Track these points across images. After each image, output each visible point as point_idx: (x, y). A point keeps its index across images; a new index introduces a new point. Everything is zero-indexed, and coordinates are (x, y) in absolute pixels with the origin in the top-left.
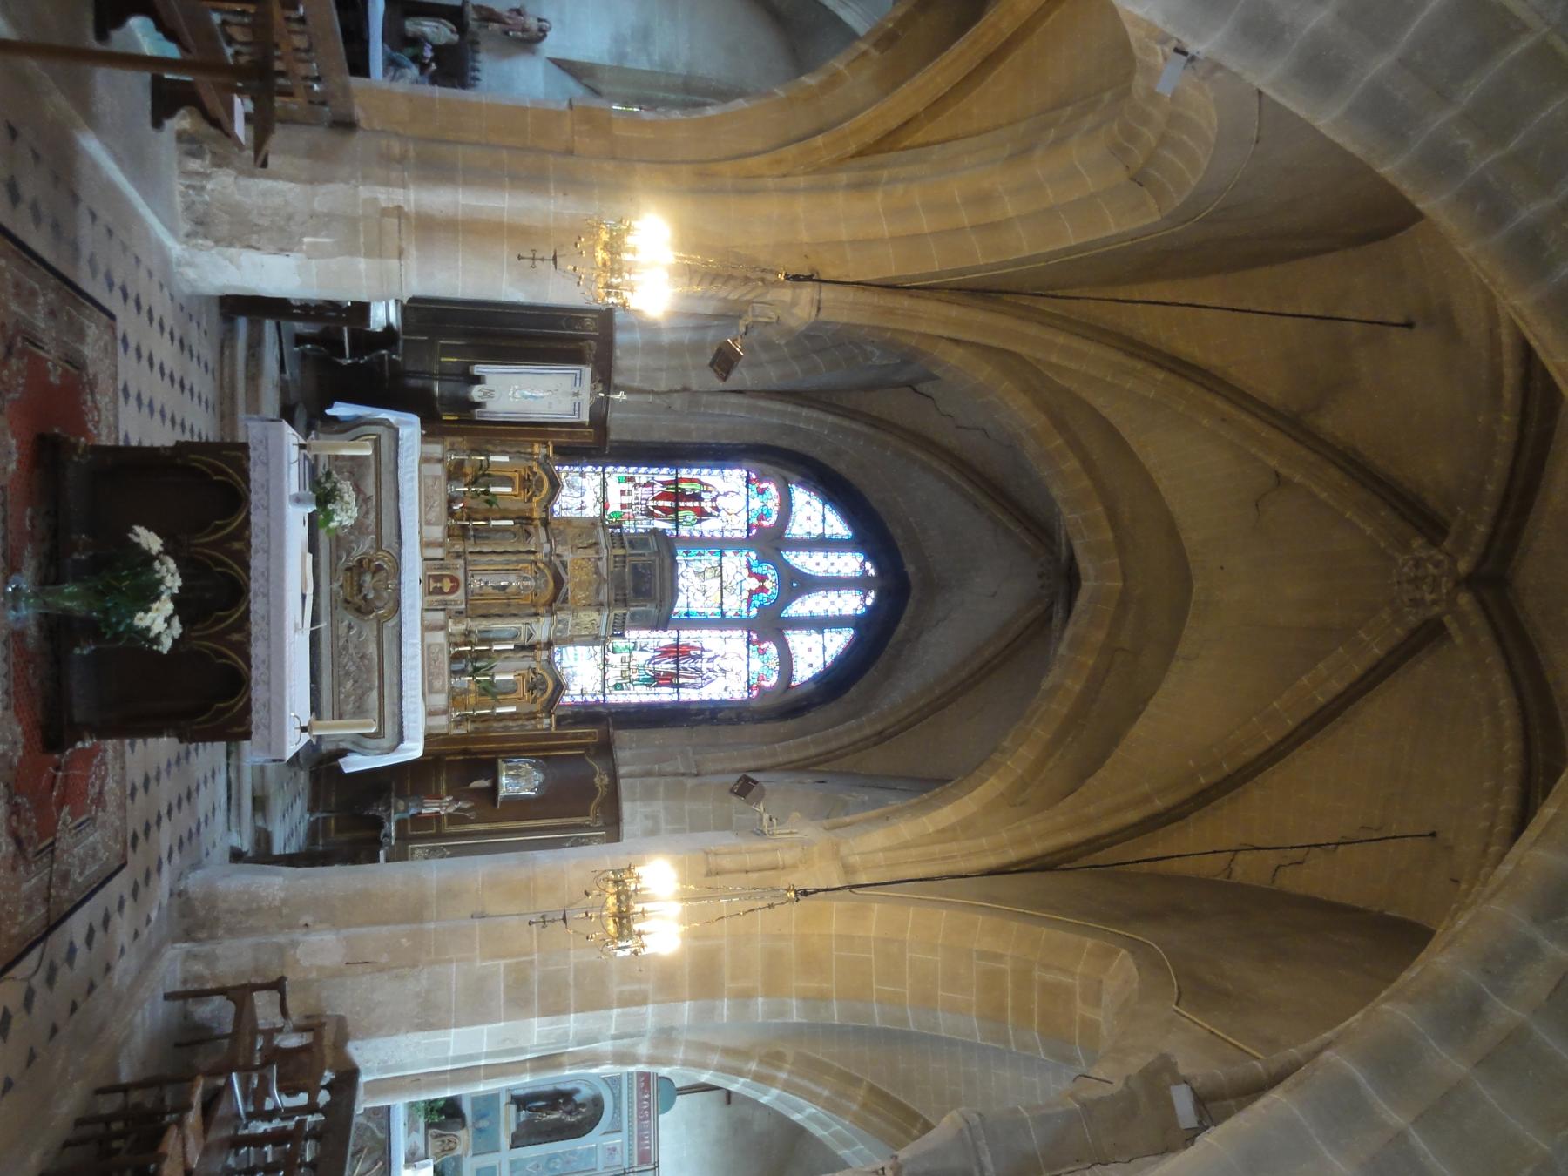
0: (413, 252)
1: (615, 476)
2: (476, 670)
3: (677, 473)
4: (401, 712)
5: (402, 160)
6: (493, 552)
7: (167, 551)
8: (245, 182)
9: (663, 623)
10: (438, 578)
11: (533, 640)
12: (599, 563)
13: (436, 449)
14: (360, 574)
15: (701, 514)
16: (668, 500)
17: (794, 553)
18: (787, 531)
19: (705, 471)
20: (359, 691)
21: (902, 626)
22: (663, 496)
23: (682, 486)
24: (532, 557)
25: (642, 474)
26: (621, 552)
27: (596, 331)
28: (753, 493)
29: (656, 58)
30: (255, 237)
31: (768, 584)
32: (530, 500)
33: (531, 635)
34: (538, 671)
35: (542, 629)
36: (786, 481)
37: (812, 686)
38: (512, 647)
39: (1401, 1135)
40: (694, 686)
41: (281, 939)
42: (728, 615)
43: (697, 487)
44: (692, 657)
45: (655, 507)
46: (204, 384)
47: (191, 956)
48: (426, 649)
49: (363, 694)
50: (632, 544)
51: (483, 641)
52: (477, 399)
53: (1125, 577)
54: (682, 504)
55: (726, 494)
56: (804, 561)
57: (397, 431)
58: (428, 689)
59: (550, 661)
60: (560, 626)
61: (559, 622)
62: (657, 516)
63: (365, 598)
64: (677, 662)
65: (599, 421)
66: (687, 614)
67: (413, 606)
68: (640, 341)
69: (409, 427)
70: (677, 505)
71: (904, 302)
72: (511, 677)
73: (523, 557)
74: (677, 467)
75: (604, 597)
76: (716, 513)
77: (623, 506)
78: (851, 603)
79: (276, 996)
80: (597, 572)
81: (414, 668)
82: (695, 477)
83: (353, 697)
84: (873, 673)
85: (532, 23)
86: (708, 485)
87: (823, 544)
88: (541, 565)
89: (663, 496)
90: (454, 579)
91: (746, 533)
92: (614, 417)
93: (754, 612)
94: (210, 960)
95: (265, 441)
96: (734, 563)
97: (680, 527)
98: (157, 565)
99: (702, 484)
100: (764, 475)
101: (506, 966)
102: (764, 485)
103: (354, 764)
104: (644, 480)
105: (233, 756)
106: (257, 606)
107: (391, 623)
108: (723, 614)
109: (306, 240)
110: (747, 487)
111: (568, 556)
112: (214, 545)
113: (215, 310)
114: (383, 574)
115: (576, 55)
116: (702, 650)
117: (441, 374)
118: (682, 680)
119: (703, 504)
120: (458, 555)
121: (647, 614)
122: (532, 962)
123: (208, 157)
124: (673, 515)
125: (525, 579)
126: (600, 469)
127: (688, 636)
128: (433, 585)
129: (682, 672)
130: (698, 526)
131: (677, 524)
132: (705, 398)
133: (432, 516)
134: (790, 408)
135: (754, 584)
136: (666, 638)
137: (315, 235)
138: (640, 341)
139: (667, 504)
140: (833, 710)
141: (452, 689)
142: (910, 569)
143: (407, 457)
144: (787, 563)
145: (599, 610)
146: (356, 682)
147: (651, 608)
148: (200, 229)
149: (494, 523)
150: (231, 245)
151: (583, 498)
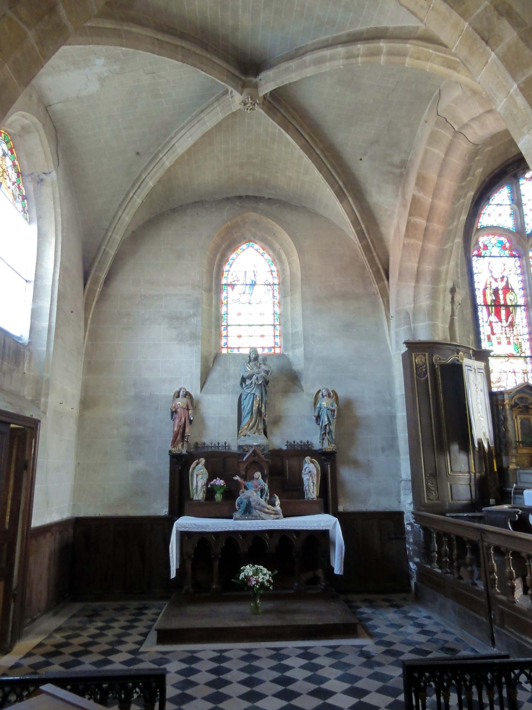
3: (480, 305)
15: (507, 289)
16: (500, 312)
17: (526, 226)
23: (489, 302)
25: (485, 330)
27: (425, 355)
28: (488, 253)
29: (191, 311)
36: (478, 230)
45: (507, 320)
54: (502, 302)
55: (491, 272)
62: (513, 319)
68: (427, 323)
70: (503, 305)
76: (505, 279)
77: (509, 343)
82: (482, 293)
85: (181, 402)
86: (486, 284)
91: (517, 258)
97: (518, 304)
99: (486, 288)
102: (481, 245)
104: (489, 328)
110: (484, 257)
115: (197, 371)
119: (500, 287)
124: (511, 308)
130: (516, 291)
138: (427, 323)
139: (503, 312)
151: (507, 371)
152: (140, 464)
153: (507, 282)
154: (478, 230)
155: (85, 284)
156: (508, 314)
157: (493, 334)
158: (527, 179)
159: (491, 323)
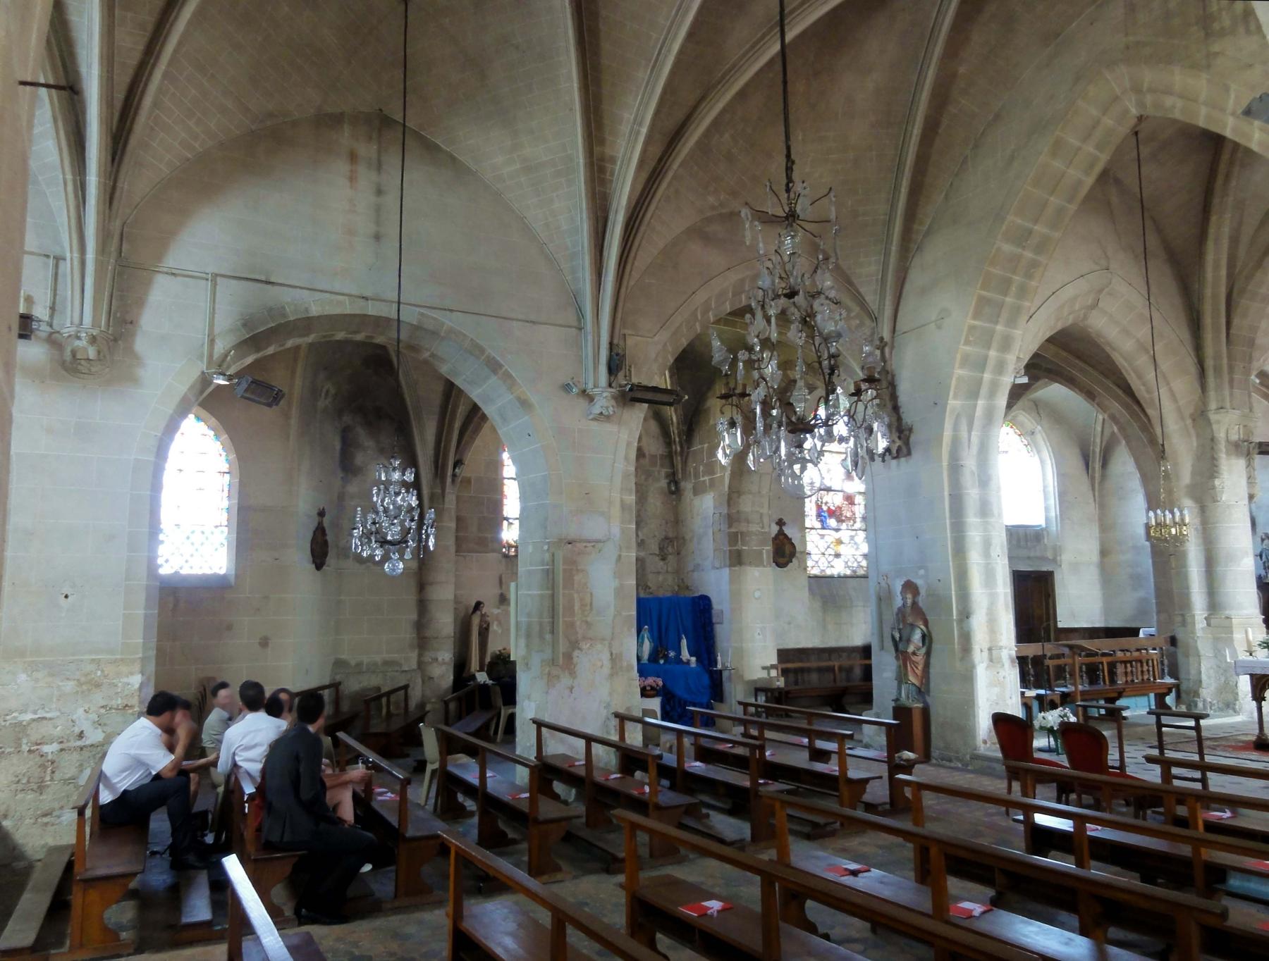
5: (1183, 615)
8: (1204, 684)
30: (1231, 683)
71: (1209, 363)
109: (1229, 660)
137: (1226, 656)
148: (1231, 706)
150: (1237, 694)
152: (1141, 594)
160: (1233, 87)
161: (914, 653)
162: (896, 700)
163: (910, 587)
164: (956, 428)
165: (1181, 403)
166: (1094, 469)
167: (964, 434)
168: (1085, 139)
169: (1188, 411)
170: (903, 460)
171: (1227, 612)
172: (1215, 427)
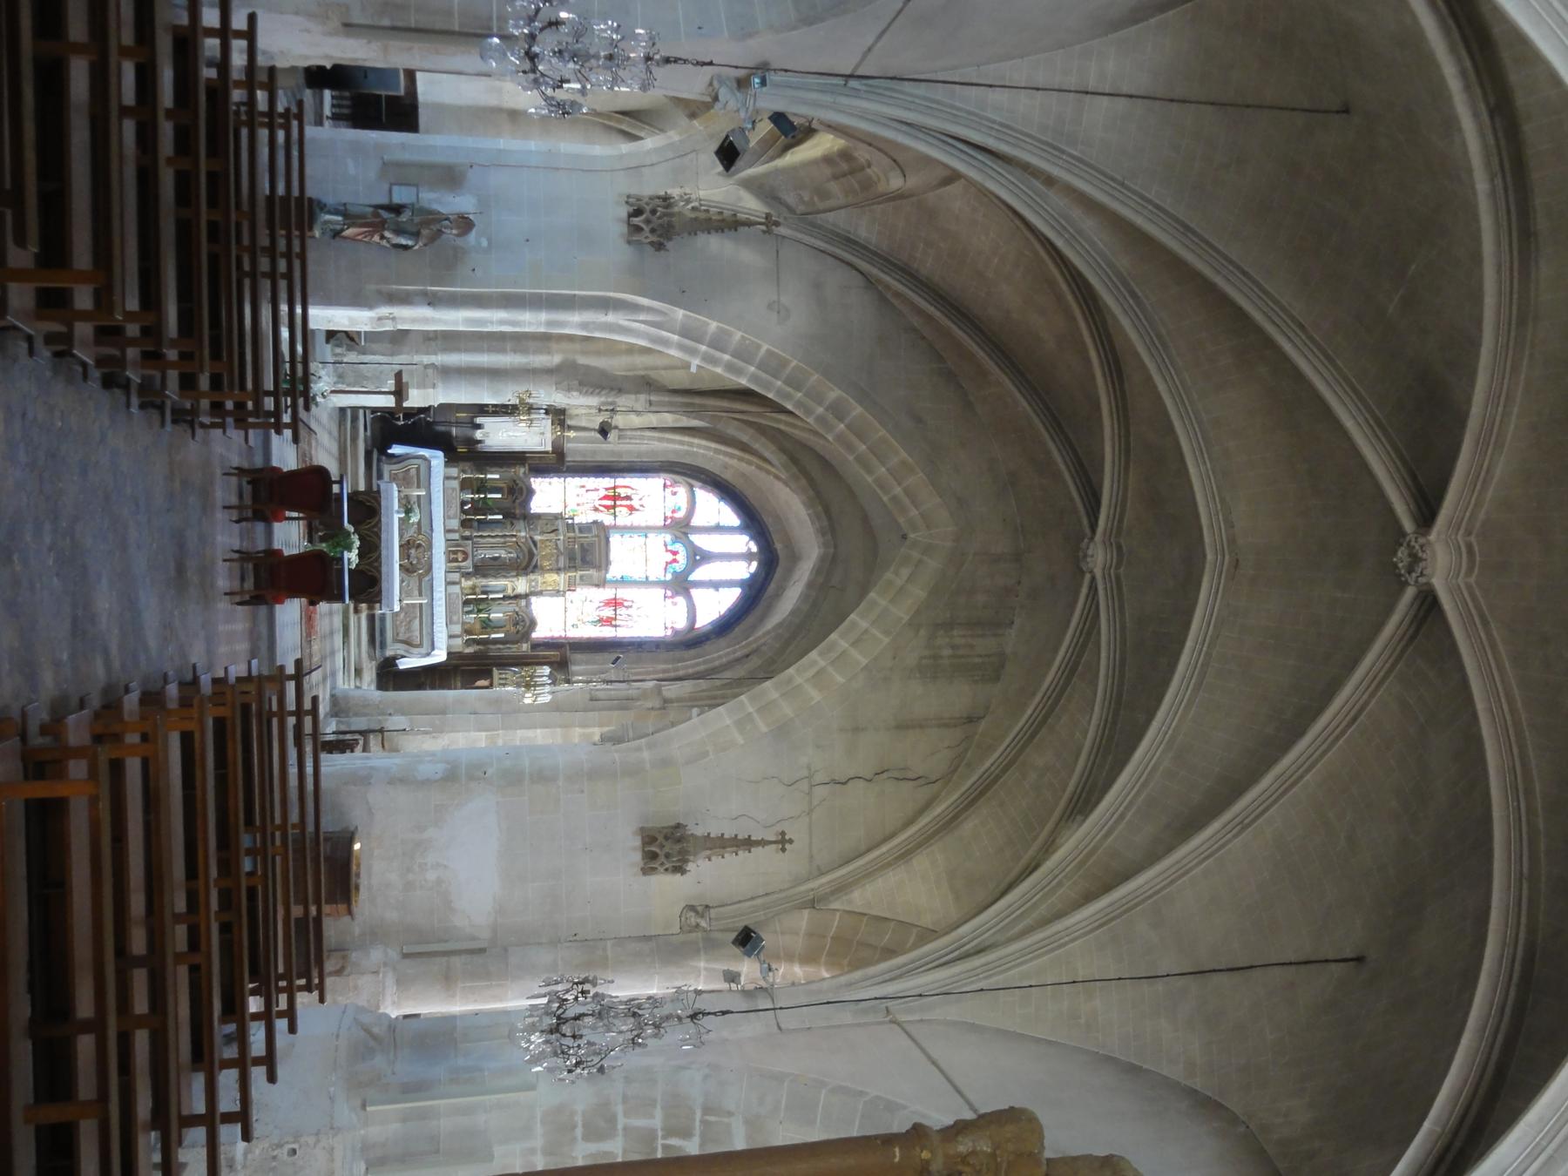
0: (440, 384)
1: (574, 482)
2: (480, 611)
4: (433, 632)
6: (489, 536)
7: (356, 531)
9: (601, 584)
10: (455, 552)
11: (516, 592)
12: (558, 542)
13: (454, 471)
14: (410, 548)
15: (631, 509)
18: (692, 521)
19: (635, 480)
20: (408, 620)
21: (772, 587)
22: (606, 497)
24: (514, 539)
25: (591, 482)
26: (572, 535)
30: (365, 382)
31: (678, 557)
32: (514, 502)
33: (514, 589)
34: (520, 613)
35: (521, 585)
36: (691, 487)
37: (710, 627)
38: (501, 596)
39: (750, 714)
40: (627, 626)
41: (380, 718)
42: (650, 579)
43: (629, 492)
44: (627, 607)
46: (334, 448)
47: (341, 722)
48: (448, 596)
49: (410, 621)
50: (581, 531)
51: (483, 593)
52: (479, 439)
53: (836, 547)
54: (618, 503)
56: (699, 540)
57: (430, 462)
58: (449, 622)
59: (528, 604)
60: (533, 584)
61: (533, 581)
63: (411, 563)
64: (615, 610)
65: (559, 451)
66: (622, 578)
67: (439, 568)
69: (437, 458)
72: (501, 615)
73: (508, 539)
74: (616, 478)
75: (561, 564)
76: (641, 508)
77: (578, 505)
78: (744, 570)
79: (380, 735)
80: (557, 548)
81: (440, 606)
83: (404, 624)
84: (750, 620)
87: (718, 529)
88: (521, 545)
89: (606, 497)
90: (464, 553)
92: (568, 446)
93: (669, 577)
94: (349, 724)
95: (386, 491)
96: (658, 541)
98: (352, 536)
99: (633, 489)
100: (676, 482)
101: (486, 736)
102: (675, 489)
103: (405, 664)
105: (346, 644)
106: (384, 553)
107: (427, 578)
108: (647, 578)
111: (537, 538)
112: (368, 529)
113: (338, 411)
114: (421, 550)
116: (633, 602)
117: (457, 423)
118: (618, 623)
120: (467, 538)
121: (591, 576)
122: (498, 734)
123: (345, 346)
124: (612, 511)
125: (510, 553)
126: (563, 479)
127: (623, 593)
128: (452, 556)
129: (618, 617)
131: (615, 516)
132: (629, 433)
133: (452, 512)
134: (686, 439)
135: (670, 557)
136: (607, 593)
140: (722, 642)
141: (464, 623)
142: (778, 546)
143: (436, 477)
144: (691, 543)
145: (557, 573)
146: (406, 614)
147: (592, 572)
148: (341, 380)
149: (490, 517)
153: (637, 510)
154: (691, 487)
155: (616, 112)
156: (607, 507)
157: (587, 491)
158: (747, 543)
159: (598, 490)
160: (886, 640)
161: (382, 237)
162: (323, 207)
163: (465, 224)
164: (649, 310)
165: (663, 372)
166: (618, 121)
167: (642, 317)
168: (906, 491)
169: (653, 374)
170: (625, 229)
171: (440, 384)
172: (633, 397)
